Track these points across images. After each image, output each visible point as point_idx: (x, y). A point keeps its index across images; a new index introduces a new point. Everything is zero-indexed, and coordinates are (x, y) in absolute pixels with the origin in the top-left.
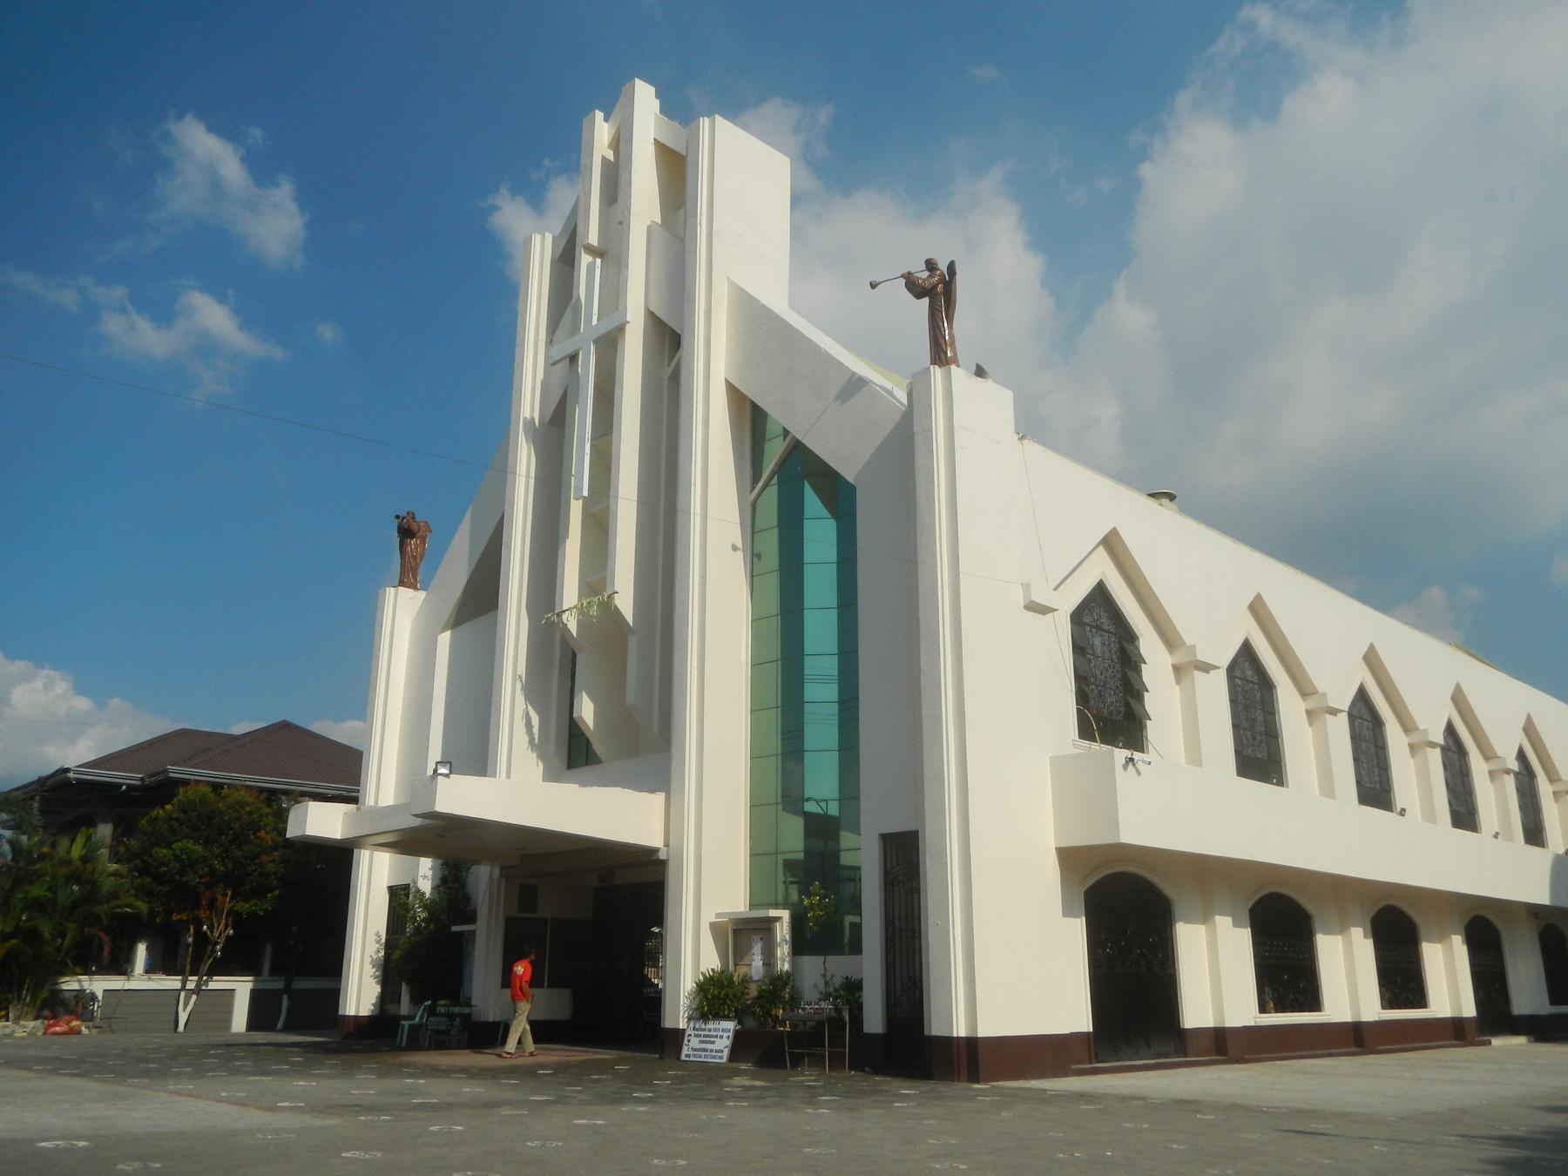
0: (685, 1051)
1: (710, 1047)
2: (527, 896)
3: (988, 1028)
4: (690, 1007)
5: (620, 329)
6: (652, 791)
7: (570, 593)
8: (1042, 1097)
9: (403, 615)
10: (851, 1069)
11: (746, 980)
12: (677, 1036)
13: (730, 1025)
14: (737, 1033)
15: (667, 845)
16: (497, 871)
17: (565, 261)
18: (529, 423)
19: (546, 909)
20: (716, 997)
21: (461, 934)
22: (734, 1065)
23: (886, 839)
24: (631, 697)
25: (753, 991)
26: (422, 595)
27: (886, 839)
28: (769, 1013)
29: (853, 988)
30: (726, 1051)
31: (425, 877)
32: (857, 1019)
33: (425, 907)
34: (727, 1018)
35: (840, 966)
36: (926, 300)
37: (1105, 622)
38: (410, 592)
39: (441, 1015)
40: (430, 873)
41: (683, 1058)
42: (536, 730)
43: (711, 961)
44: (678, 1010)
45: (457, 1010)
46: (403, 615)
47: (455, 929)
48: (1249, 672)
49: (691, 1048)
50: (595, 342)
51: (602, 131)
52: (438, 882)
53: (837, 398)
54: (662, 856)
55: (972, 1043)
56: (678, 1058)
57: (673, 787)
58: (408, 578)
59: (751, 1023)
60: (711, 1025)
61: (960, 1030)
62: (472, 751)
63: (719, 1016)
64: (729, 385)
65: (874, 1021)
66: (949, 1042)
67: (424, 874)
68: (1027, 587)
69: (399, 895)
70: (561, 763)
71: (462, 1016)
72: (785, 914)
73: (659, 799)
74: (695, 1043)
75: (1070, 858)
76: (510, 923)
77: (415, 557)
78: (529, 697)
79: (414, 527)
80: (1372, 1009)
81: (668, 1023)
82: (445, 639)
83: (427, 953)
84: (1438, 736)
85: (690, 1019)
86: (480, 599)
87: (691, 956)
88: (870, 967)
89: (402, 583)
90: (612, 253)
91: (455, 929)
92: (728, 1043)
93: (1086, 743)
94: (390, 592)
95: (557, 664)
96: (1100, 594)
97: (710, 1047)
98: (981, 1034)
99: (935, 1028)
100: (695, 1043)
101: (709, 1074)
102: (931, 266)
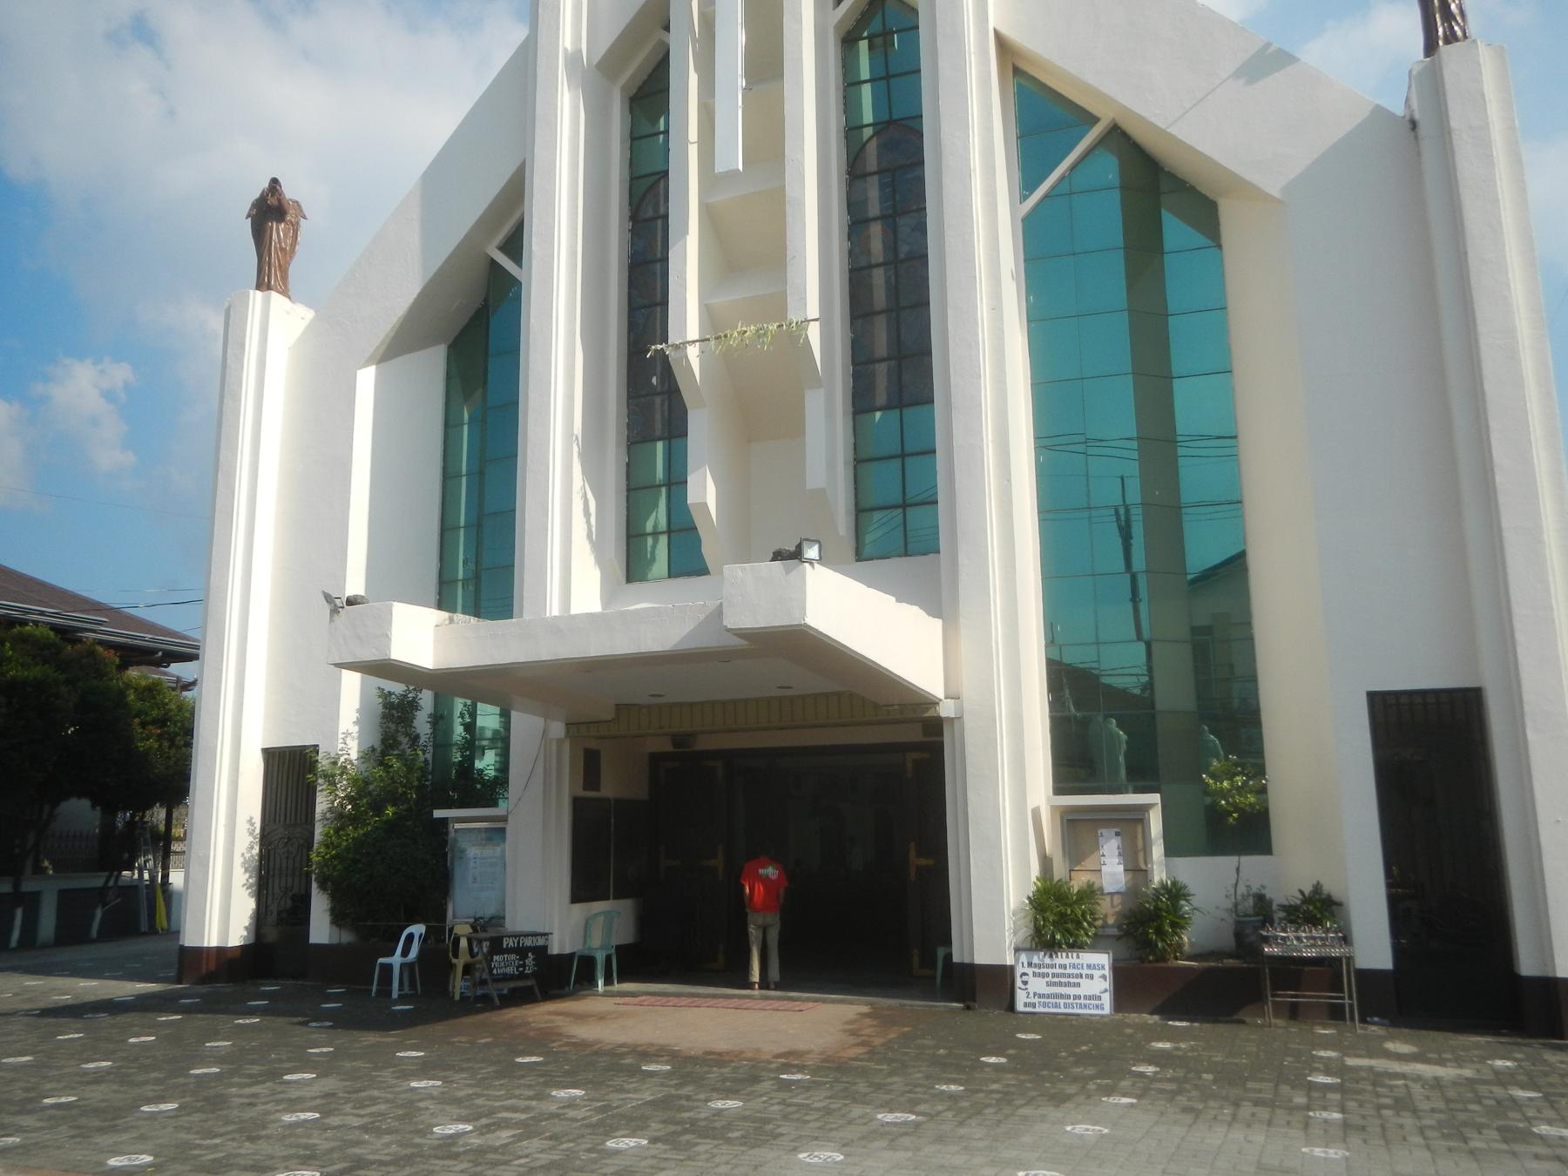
0: (1021, 1000)
4: (1015, 933)
9: (278, 328)
12: (999, 981)
13: (1103, 959)
16: (558, 729)
18: (573, 59)
20: (1058, 919)
22: (1119, 1016)
30: (1107, 1000)
31: (347, 734)
39: (510, 951)
40: (355, 729)
41: (1020, 1007)
42: (593, 520)
47: (438, 814)
52: (375, 740)
53: (1238, 74)
54: (946, 710)
56: (1011, 1007)
57: (964, 609)
60: (1062, 959)
63: (1076, 946)
65: (1373, 946)
70: (620, 572)
73: (937, 624)
76: (578, 804)
77: (282, 249)
78: (586, 472)
82: (367, 378)
85: (1017, 950)
89: (262, 284)
91: (438, 814)
92: (1107, 985)
94: (257, 297)
100: (1038, 985)
101: (1066, 1030)
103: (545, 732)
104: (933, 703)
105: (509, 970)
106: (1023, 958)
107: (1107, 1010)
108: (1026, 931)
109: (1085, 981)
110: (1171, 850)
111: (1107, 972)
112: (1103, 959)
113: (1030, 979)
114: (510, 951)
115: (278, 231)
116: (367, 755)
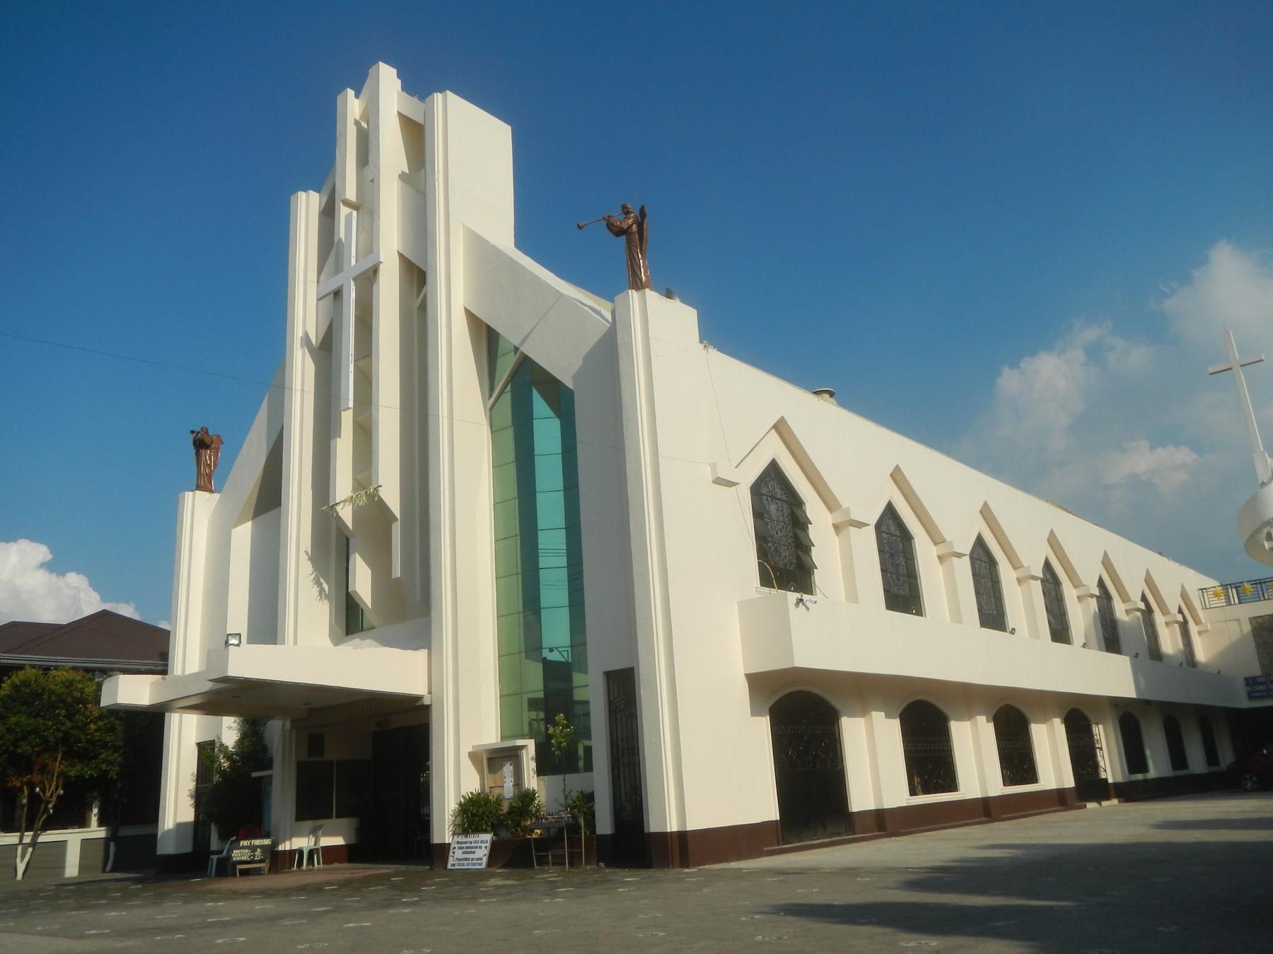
0: (451, 861)
1: (471, 856)
2: (315, 743)
3: (696, 823)
5: (375, 270)
6: (416, 649)
7: (343, 485)
8: (738, 875)
9: (199, 512)
10: (587, 864)
11: (499, 801)
12: (444, 849)
13: (488, 837)
14: (494, 845)
15: (430, 693)
16: (288, 724)
17: (328, 213)
19: (332, 754)
20: (475, 814)
21: (262, 778)
22: (492, 869)
23: (611, 676)
24: (397, 572)
25: (505, 807)
26: (216, 496)
27: (611, 676)
28: (518, 825)
29: (589, 798)
30: (485, 860)
32: (591, 823)
33: (229, 757)
34: (485, 831)
35: (576, 782)
36: (623, 238)
37: (779, 492)
38: (206, 495)
39: (244, 847)
41: (449, 867)
43: (472, 783)
44: (444, 829)
45: (257, 842)
46: (199, 512)
47: (254, 775)
48: (777, 490)
49: (455, 859)
50: (355, 279)
51: (352, 105)
54: (426, 702)
55: (683, 837)
58: (204, 483)
59: (504, 834)
60: (472, 838)
61: (673, 826)
62: (266, 626)
63: (478, 830)
64: (468, 313)
65: (604, 825)
66: (664, 836)
67: (229, 731)
68: (713, 466)
69: (206, 750)
70: (341, 631)
71: (261, 847)
72: (530, 744)
73: (423, 654)
74: (459, 854)
75: (757, 682)
79: (207, 440)
80: (996, 787)
81: (436, 840)
83: (232, 795)
84: (966, 546)
85: (454, 834)
86: (269, 497)
87: (455, 780)
88: (600, 781)
89: (199, 488)
90: (366, 206)
91: (254, 775)
92: (486, 852)
93: (767, 590)
94: (189, 495)
95: (334, 547)
96: (773, 472)
97: (471, 856)
98: (690, 828)
99: (653, 826)
101: (471, 877)
102: (627, 212)
103: (283, 726)
104: (419, 698)
105: (244, 858)
106: (457, 839)
107: (484, 866)
108: (458, 821)
109: (474, 851)
110: (541, 771)
111: (488, 845)
112: (488, 837)
113: (457, 851)
114: (244, 847)
115: (207, 455)
116: (240, 743)
